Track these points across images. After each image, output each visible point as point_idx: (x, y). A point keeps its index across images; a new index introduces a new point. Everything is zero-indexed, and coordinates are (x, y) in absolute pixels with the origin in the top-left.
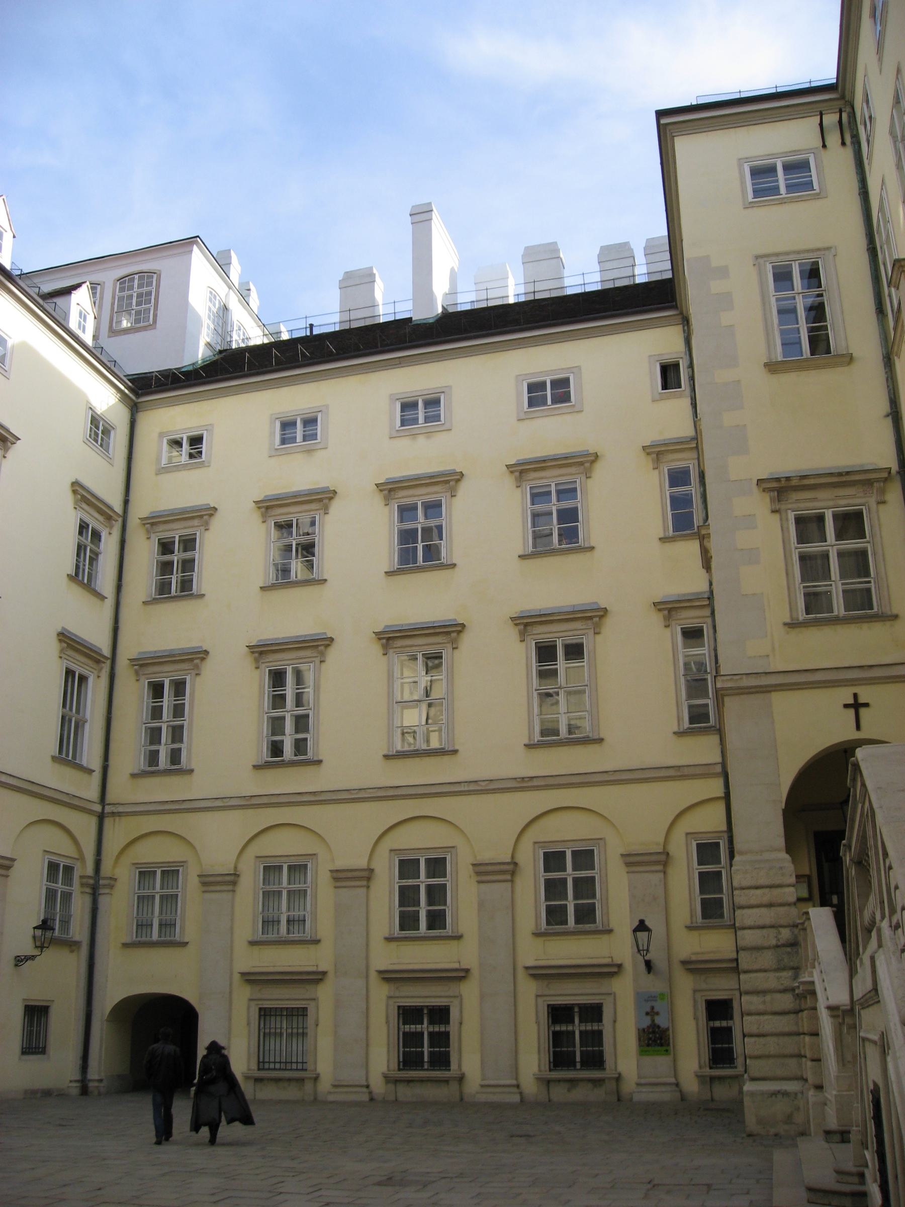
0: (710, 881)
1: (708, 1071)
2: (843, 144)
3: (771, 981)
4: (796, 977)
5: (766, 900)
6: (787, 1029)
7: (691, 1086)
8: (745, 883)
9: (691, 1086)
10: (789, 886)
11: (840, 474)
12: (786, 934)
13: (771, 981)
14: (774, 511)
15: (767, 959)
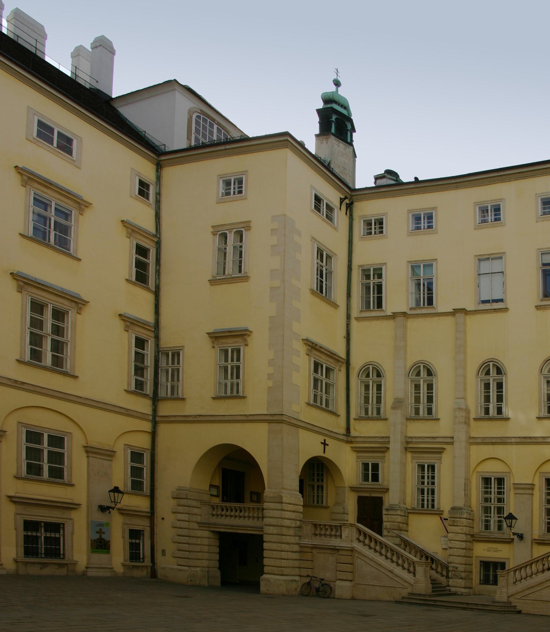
0: (136, 472)
1: (128, 563)
2: (346, 214)
3: (293, 540)
4: (300, 539)
5: (293, 509)
6: (296, 558)
7: (119, 569)
8: (287, 502)
9: (119, 569)
10: (301, 505)
11: (332, 353)
12: (298, 523)
13: (293, 540)
14: (308, 355)
15: (292, 532)
